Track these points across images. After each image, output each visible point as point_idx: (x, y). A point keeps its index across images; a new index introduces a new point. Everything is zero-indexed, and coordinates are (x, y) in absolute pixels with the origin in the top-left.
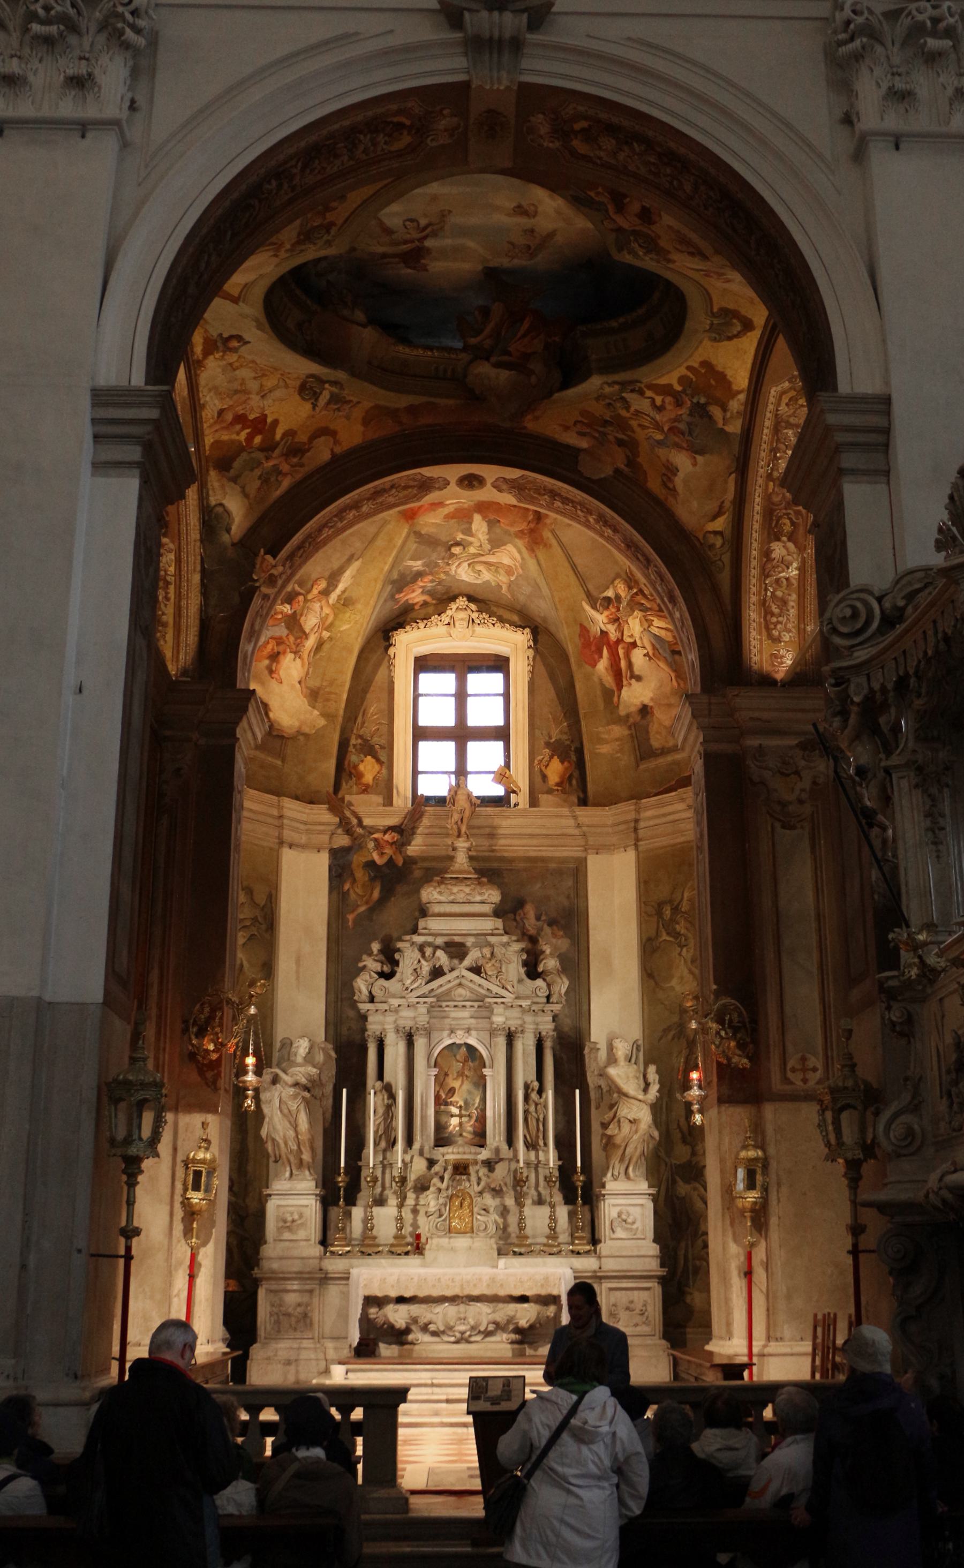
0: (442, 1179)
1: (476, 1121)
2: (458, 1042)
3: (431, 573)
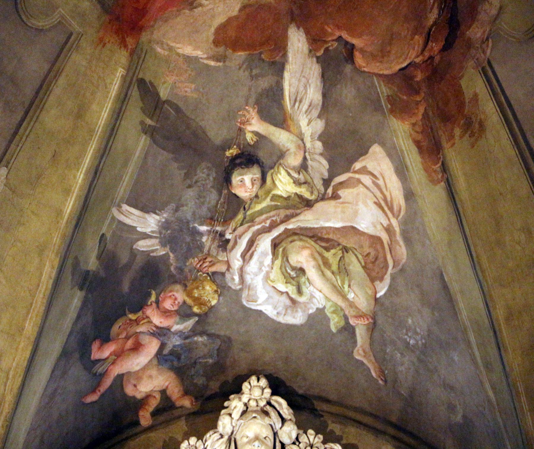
3: (183, 280)
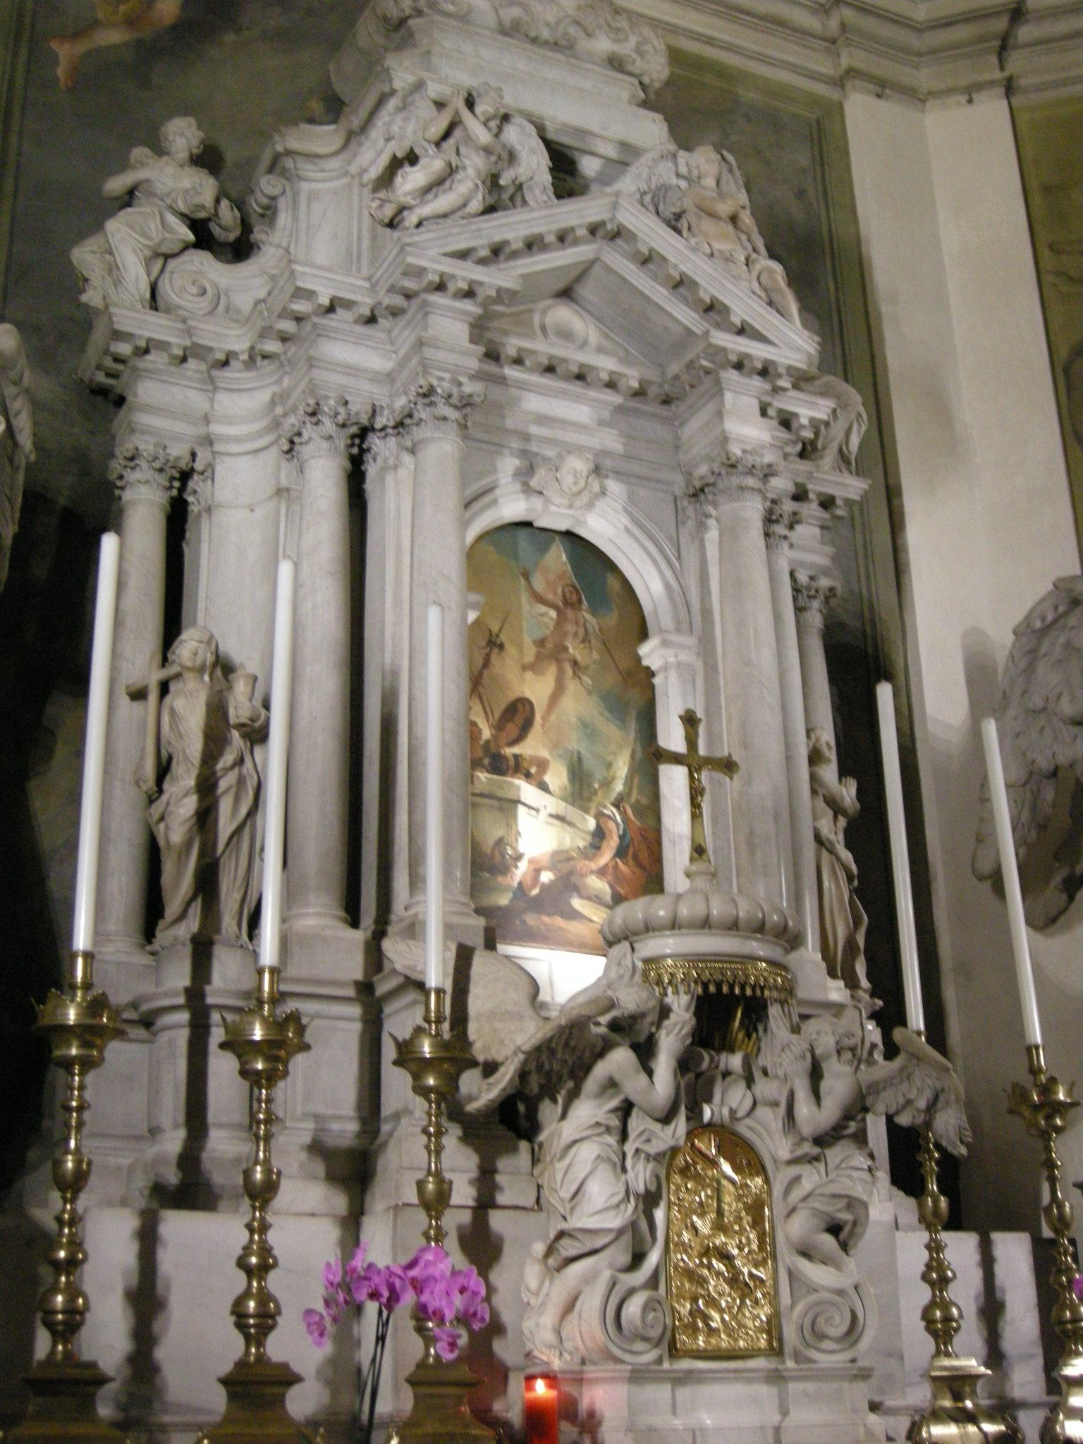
0: (645, 1052)
1: (621, 853)
2: (554, 517)
